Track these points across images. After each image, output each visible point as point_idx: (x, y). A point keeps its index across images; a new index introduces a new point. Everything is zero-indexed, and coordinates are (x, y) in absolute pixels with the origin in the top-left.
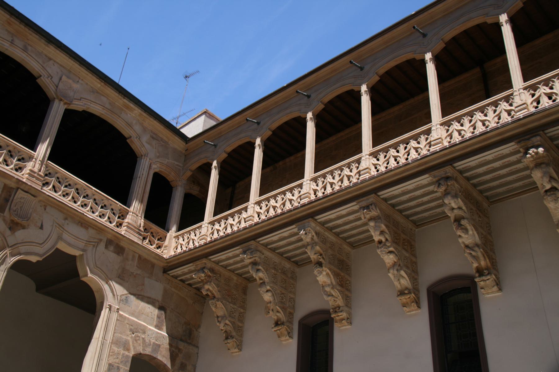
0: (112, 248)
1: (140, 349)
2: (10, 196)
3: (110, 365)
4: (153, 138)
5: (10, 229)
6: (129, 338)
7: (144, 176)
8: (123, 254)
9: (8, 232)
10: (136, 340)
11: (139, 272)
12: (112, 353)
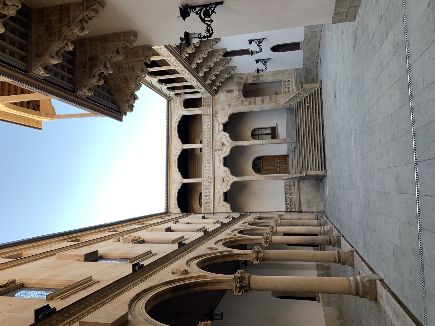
0: (217, 115)
1: (242, 96)
6: (239, 101)
9: (226, 146)
10: (240, 98)
11: (220, 104)
12: (246, 105)
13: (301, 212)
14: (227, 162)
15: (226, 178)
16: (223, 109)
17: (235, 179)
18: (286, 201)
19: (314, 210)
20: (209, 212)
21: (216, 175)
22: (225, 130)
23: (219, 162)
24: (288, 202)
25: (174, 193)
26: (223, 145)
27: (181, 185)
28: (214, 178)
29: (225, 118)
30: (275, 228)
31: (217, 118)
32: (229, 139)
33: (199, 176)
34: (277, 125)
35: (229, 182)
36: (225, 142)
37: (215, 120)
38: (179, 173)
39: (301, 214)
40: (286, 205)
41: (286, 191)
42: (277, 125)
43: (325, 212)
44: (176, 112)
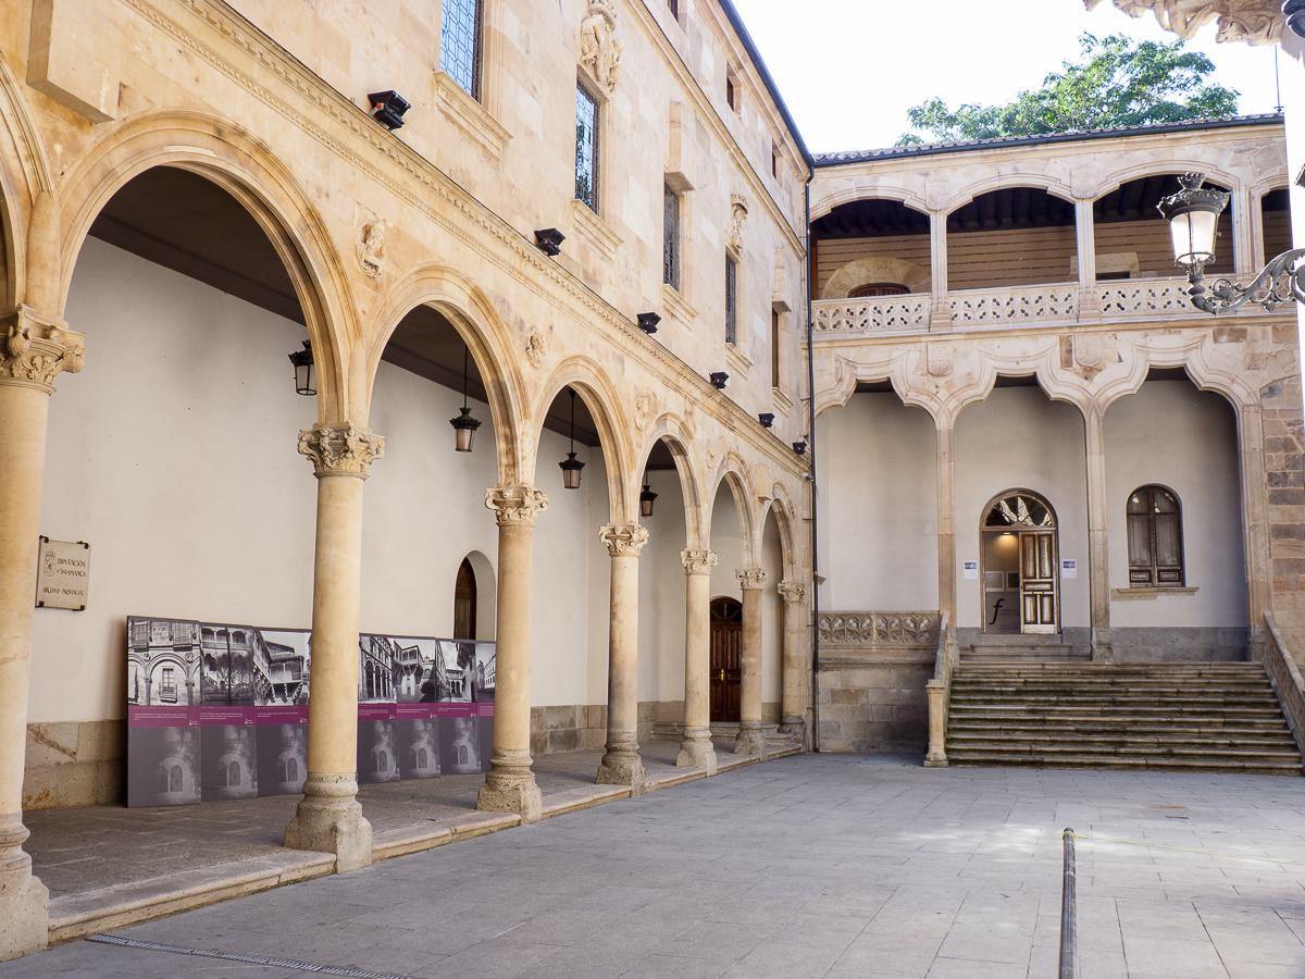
0: (1225, 338)
2: (1071, 345)
3: (1270, 475)
4: (1240, 152)
5: (1086, 378)
7: (1244, 217)
8: (1245, 338)
11: (1280, 347)
13: (816, 666)
14: (1022, 387)
15: (949, 385)
16: (1253, 364)
17: (943, 423)
18: (859, 617)
19: (825, 715)
20: (817, 326)
21: (962, 345)
22: (1156, 375)
23: (1017, 356)
24: (853, 625)
25: (888, 184)
26: (1089, 372)
27: (919, 206)
28: (955, 339)
29: (1210, 371)
30: (706, 569)
31: (1209, 341)
32: (1112, 393)
33: (955, 283)
34: (1192, 591)
35: (933, 397)
36: (1099, 378)
37: (1203, 331)
38: (967, 198)
39: (810, 666)
40: (844, 616)
41: (896, 615)
42: (1192, 591)
43: (816, 750)
44: (1244, 157)
